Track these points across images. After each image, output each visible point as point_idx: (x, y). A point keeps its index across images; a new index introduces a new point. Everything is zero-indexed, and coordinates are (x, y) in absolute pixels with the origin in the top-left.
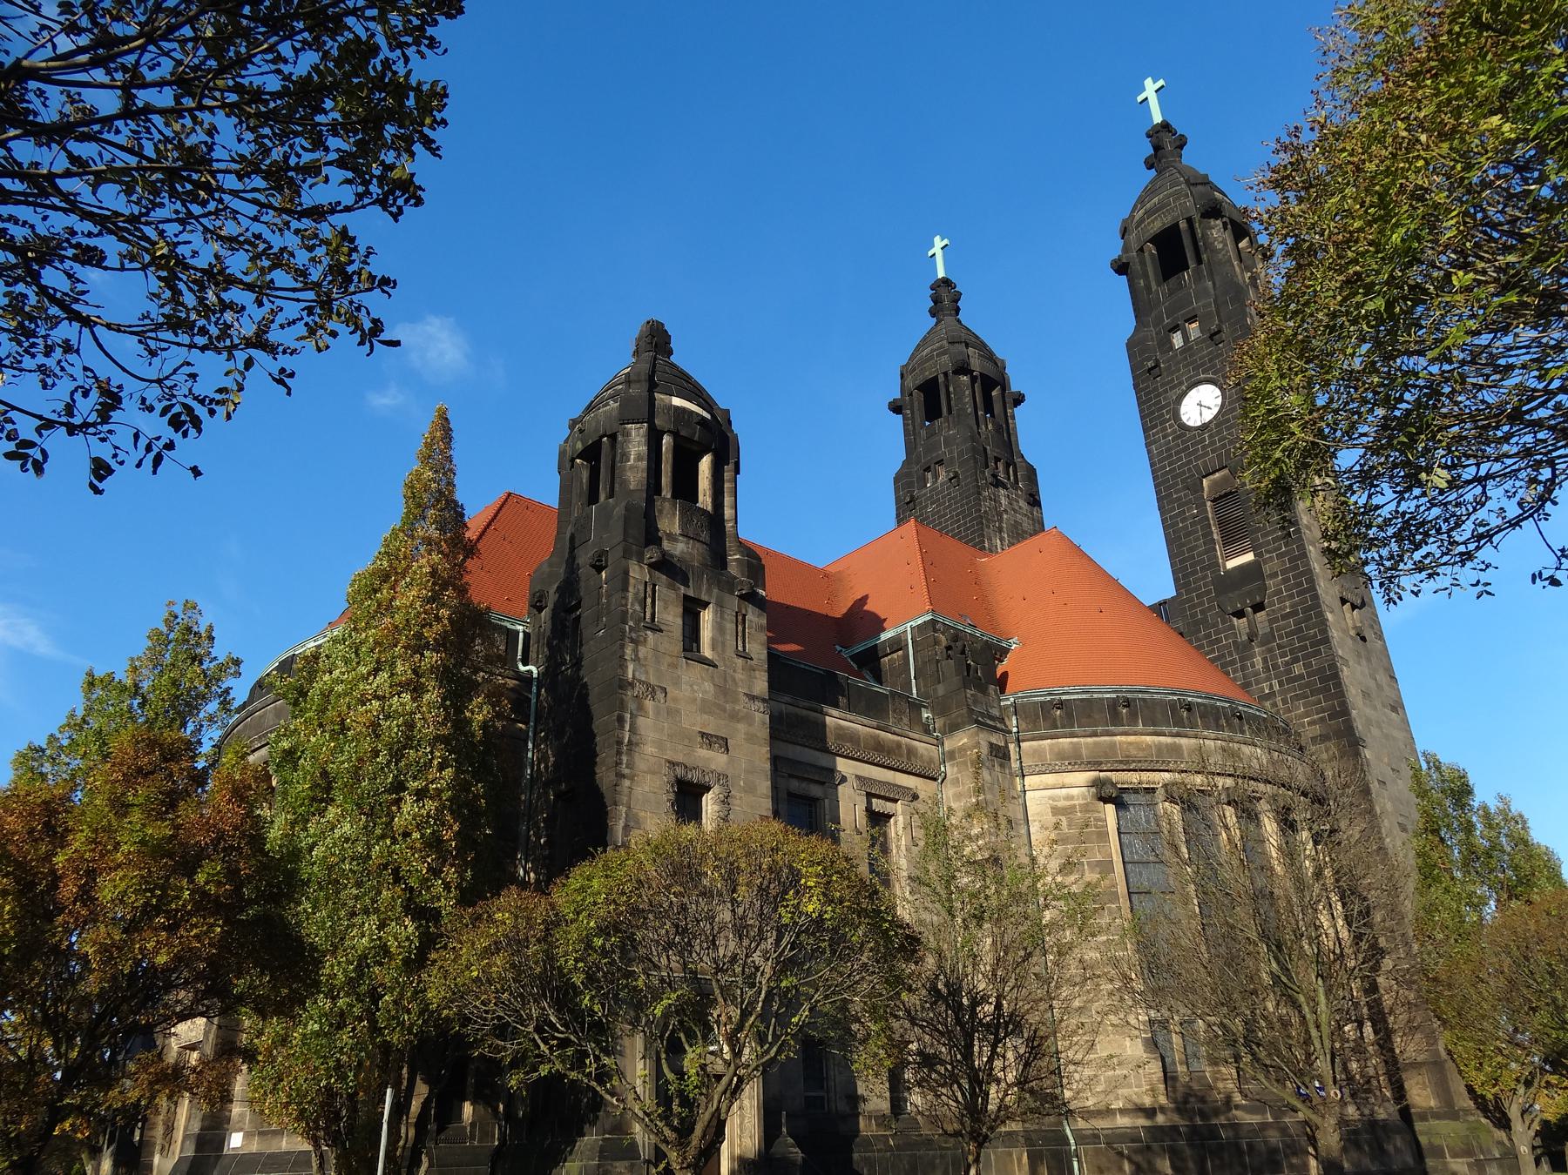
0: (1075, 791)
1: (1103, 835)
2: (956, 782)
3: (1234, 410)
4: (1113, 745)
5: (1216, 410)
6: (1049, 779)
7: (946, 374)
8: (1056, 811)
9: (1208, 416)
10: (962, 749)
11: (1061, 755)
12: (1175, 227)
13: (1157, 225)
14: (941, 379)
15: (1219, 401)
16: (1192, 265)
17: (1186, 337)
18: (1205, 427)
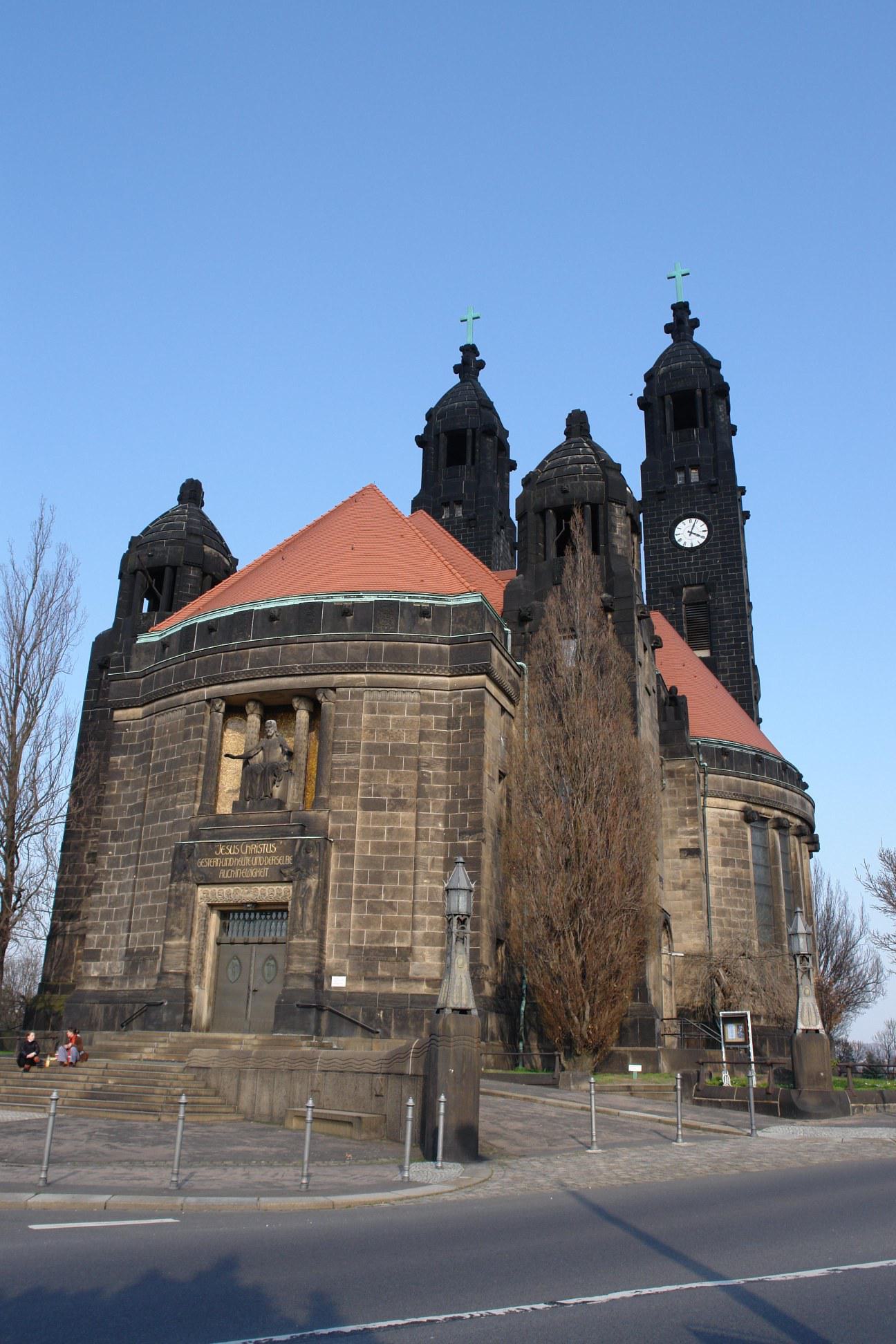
0: (733, 813)
1: (745, 844)
2: (673, 793)
3: (716, 545)
4: (757, 787)
5: (702, 541)
6: (720, 802)
7: (474, 430)
8: (722, 824)
9: (696, 542)
10: (680, 772)
11: (729, 787)
12: (693, 392)
13: (680, 385)
14: (469, 433)
15: (706, 534)
16: (701, 426)
17: (687, 477)
18: (692, 550)
